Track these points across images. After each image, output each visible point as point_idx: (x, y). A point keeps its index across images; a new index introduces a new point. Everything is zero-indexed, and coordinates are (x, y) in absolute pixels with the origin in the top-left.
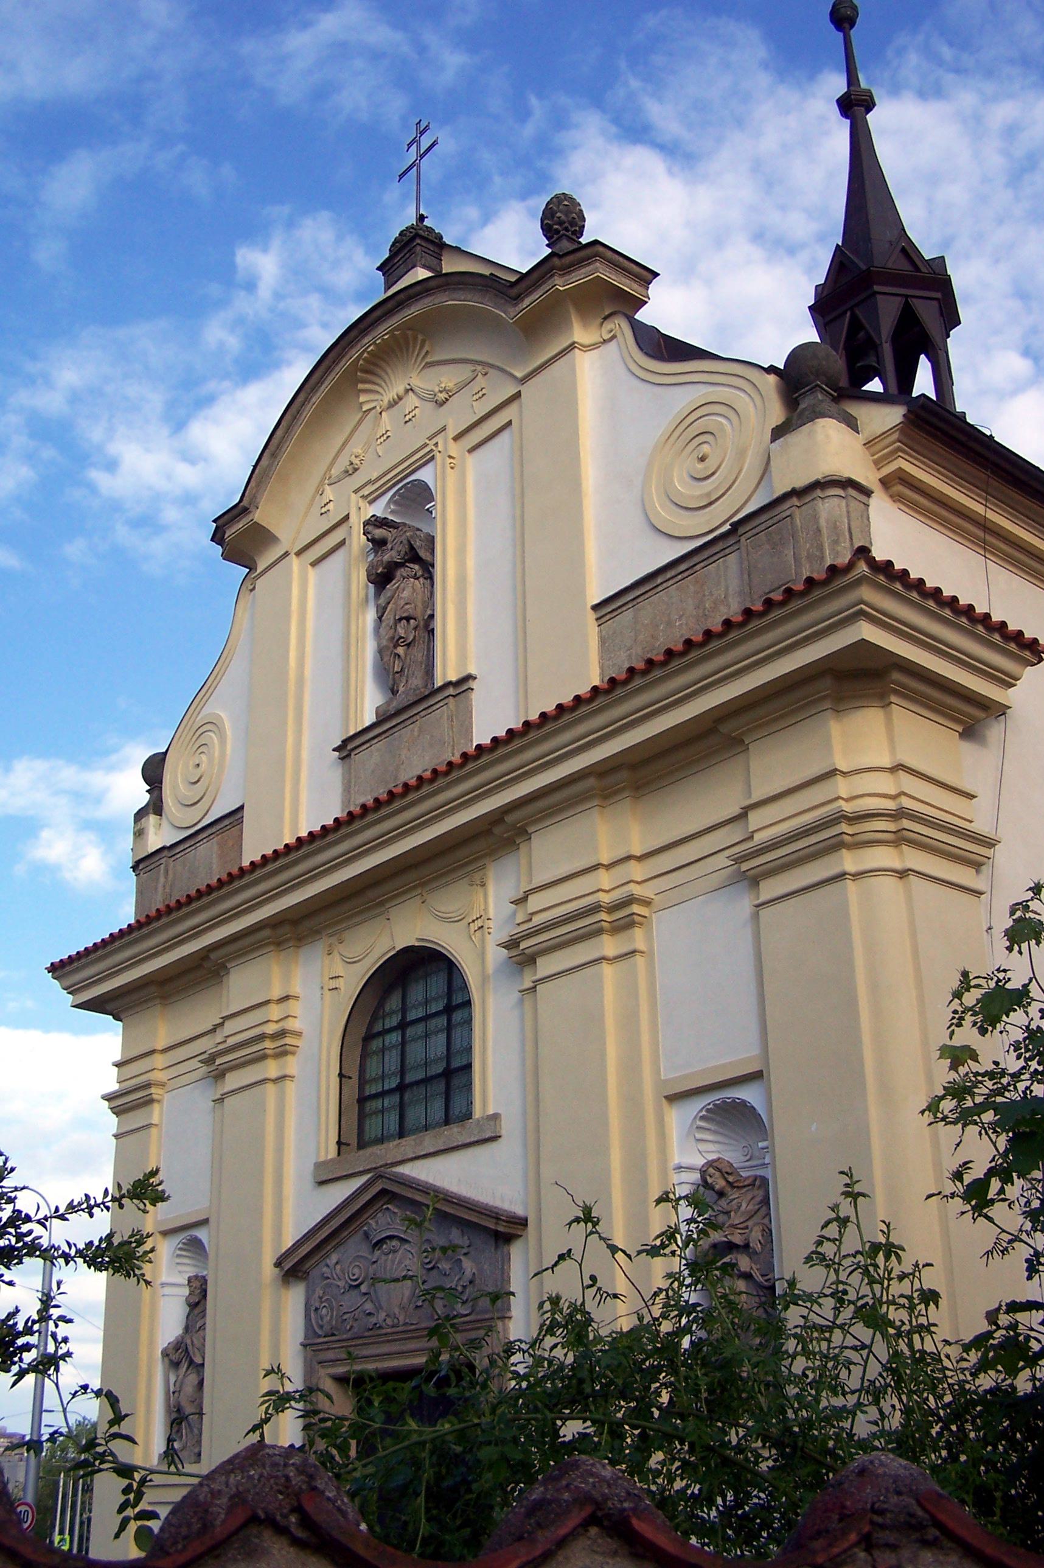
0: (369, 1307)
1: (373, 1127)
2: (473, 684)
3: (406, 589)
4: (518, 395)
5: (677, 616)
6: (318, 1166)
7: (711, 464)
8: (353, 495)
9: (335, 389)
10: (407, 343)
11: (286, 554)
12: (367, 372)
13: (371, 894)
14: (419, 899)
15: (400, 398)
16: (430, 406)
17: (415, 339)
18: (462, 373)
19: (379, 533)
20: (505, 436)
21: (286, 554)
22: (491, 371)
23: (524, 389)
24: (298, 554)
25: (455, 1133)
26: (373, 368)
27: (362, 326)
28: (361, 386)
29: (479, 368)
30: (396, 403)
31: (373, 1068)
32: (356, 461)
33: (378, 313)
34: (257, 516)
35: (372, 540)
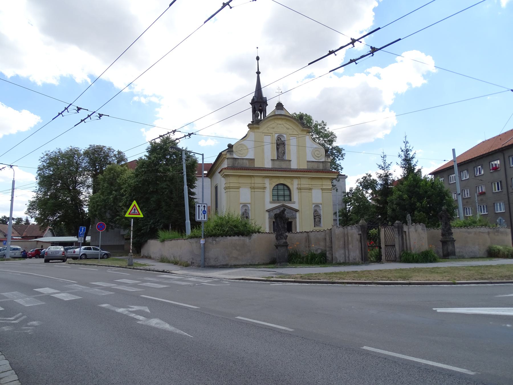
5: (315, 166)
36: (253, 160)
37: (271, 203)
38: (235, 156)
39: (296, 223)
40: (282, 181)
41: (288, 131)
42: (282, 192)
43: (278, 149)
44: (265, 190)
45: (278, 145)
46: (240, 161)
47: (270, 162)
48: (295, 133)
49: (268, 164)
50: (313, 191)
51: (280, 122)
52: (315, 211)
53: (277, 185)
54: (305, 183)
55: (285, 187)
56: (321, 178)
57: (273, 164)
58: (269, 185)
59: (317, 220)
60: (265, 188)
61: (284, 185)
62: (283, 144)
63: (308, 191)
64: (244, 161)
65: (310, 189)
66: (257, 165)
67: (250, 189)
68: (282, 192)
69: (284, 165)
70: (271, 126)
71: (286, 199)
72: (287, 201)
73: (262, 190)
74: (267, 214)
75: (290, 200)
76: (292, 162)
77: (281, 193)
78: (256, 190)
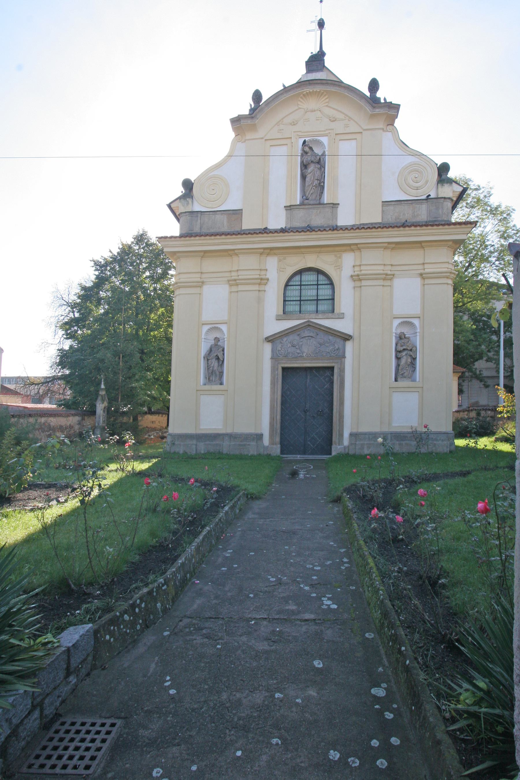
6: (277, 316)
12: (304, 95)
15: (315, 111)
17: (326, 95)
27: (311, 82)
32: (295, 122)
33: (319, 82)
36: (237, 213)
37: (279, 318)
38: (197, 208)
39: (342, 370)
40: (311, 261)
42: (310, 288)
44: (267, 288)
45: (304, 166)
47: (283, 213)
48: (353, 128)
49: (277, 220)
50: (397, 282)
52: (401, 337)
53: (300, 272)
54: (374, 260)
55: (321, 277)
56: (420, 245)
57: (289, 218)
59: (403, 361)
61: (319, 272)
62: (320, 162)
63: (381, 282)
64: (218, 217)
65: (388, 277)
67: (227, 286)
68: (310, 288)
69: (318, 219)
71: (320, 308)
72: (323, 312)
74: (268, 348)
75: (333, 311)
76: (340, 209)
77: (310, 293)
78: (241, 288)
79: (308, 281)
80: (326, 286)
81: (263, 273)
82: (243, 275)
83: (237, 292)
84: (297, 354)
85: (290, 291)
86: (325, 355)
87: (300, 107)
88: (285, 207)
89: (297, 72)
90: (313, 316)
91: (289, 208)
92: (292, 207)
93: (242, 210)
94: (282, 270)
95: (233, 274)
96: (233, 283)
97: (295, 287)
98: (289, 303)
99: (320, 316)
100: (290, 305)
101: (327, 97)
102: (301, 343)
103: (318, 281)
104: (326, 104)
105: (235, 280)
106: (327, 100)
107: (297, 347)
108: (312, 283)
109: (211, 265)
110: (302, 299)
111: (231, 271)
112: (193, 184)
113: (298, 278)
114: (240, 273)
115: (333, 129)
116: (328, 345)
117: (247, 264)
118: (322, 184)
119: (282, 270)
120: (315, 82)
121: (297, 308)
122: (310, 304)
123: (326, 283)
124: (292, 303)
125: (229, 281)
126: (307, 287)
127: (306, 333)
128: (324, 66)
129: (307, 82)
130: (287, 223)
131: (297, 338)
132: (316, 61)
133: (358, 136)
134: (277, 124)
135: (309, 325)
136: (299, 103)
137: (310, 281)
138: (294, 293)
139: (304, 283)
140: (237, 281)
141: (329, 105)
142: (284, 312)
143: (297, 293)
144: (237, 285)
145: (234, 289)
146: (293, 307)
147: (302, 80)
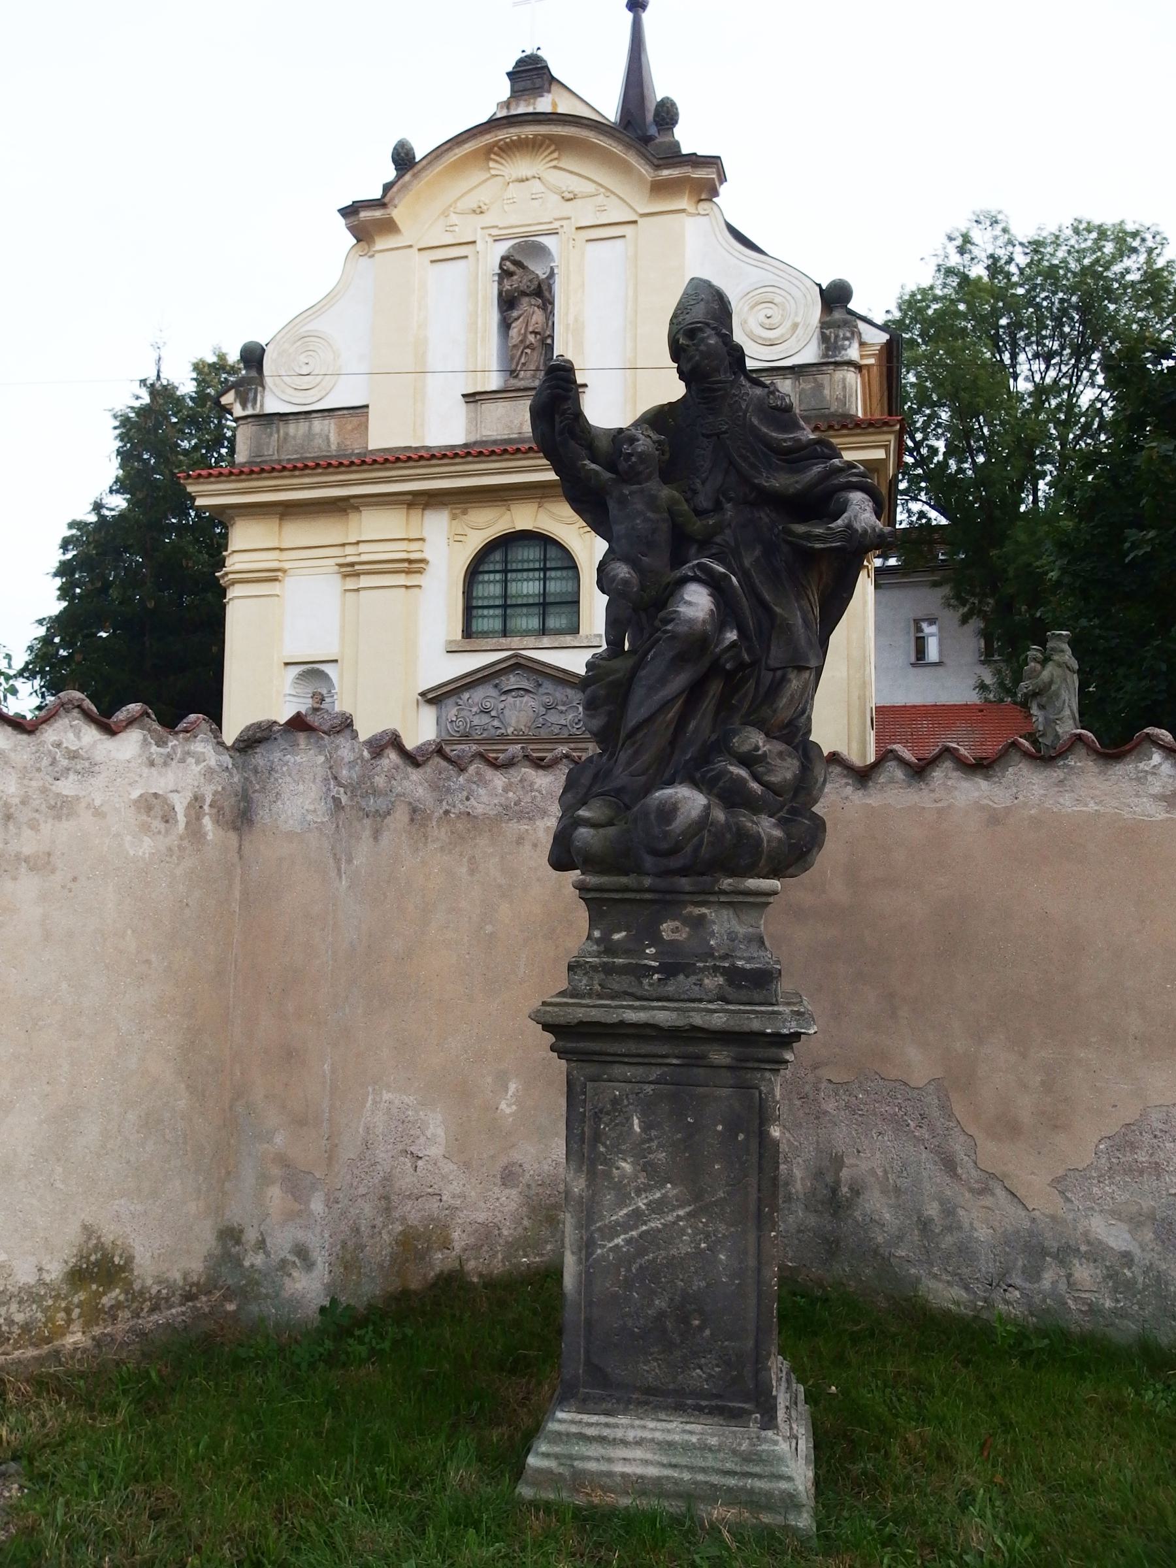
0: (496, 723)
1: (480, 625)
2: (586, 390)
3: (529, 313)
4: (635, 222)
7: (774, 321)
8: (479, 230)
9: (474, 153)
10: (541, 146)
11: (411, 246)
12: (500, 148)
13: (501, 494)
14: (536, 505)
15: (527, 179)
16: (557, 198)
17: (548, 146)
18: (590, 188)
19: (508, 265)
20: (619, 242)
21: (411, 246)
22: (613, 197)
23: (640, 221)
24: (420, 250)
25: (568, 640)
26: (508, 149)
28: (493, 156)
29: (603, 190)
30: (522, 181)
31: (479, 590)
32: (484, 208)
33: (530, 118)
34: (397, 214)
35: (501, 267)
38: (272, 405)
40: (523, 518)
41: (567, 209)
43: (505, 325)
45: (508, 303)
46: (295, 430)
47: (461, 409)
49: (448, 427)
51: (522, 166)
57: (473, 422)
58: (447, 546)
60: (414, 566)
62: (542, 293)
64: (318, 425)
66: (382, 435)
67: (337, 578)
70: (470, 202)
73: (401, 579)
77: (529, 588)
78: (365, 581)
79: (522, 561)
80: (565, 573)
81: (415, 546)
82: (370, 553)
83: (357, 590)
84: (493, 731)
85: (480, 587)
86: (556, 731)
87: (493, 172)
88: (464, 396)
89: (490, 95)
90: (530, 641)
91: (472, 398)
92: (478, 398)
93: (367, 406)
94: (459, 538)
95: (349, 550)
96: (350, 570)
97: (492, 576)
98: (480, 612)
99: (546, 641)
100: (483, 617)
101: (553, 148)
102: (501, 706)
103: (545, 560)
104: (554, 163)
105: (352, 564)
106: (555, 155)
107: (493, 713)
108: (531, 566)
109: (299, 533)
110: (509, 602)
111: (343, 545)
112: (264, 350)
113: (497, 556)
114: (363, 548)
115: (569, 218)
116: (564, 708)
117: (379, 530)
118: (549, 341)
119: (459, 538)
120: (520, 119)
121: (497, 624)
122: (527, 615)
123: (566, 565)
124: (486, 612)
125: (341, 565)
126: (519, 575)
127: (512, 681)
128: (553, 78)
129: (504, 121)
130: (468, 432)
131: (492, 692)
132: (531, 74)
133: (627, 230)
134: (443, 213)
135: (518, 665)
136: (492, 164)
137: (528, 561)
138: (490, 589)
139: (514, 566)
140: (357, 567)
141: (561, 165)
142: (468, 633)
143: (496, 590)
144: (357, 575)
145: (351, 584)
146: (489, 622)
147: (499, 115)
